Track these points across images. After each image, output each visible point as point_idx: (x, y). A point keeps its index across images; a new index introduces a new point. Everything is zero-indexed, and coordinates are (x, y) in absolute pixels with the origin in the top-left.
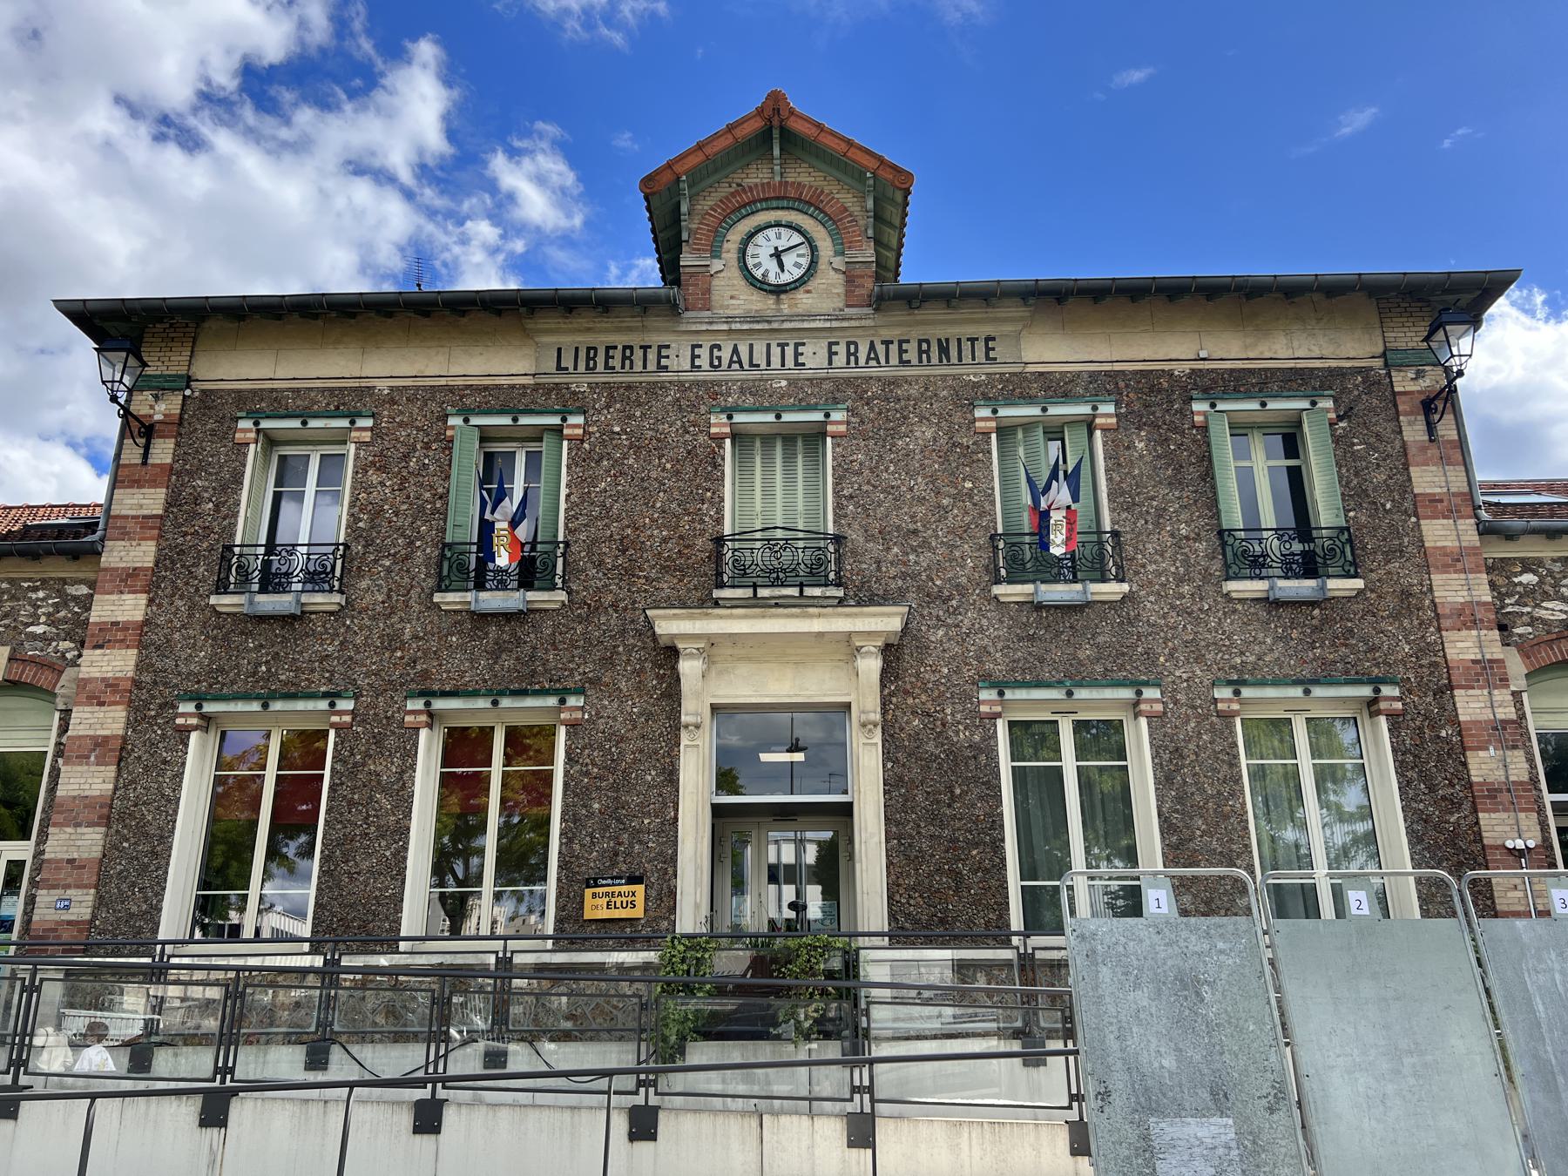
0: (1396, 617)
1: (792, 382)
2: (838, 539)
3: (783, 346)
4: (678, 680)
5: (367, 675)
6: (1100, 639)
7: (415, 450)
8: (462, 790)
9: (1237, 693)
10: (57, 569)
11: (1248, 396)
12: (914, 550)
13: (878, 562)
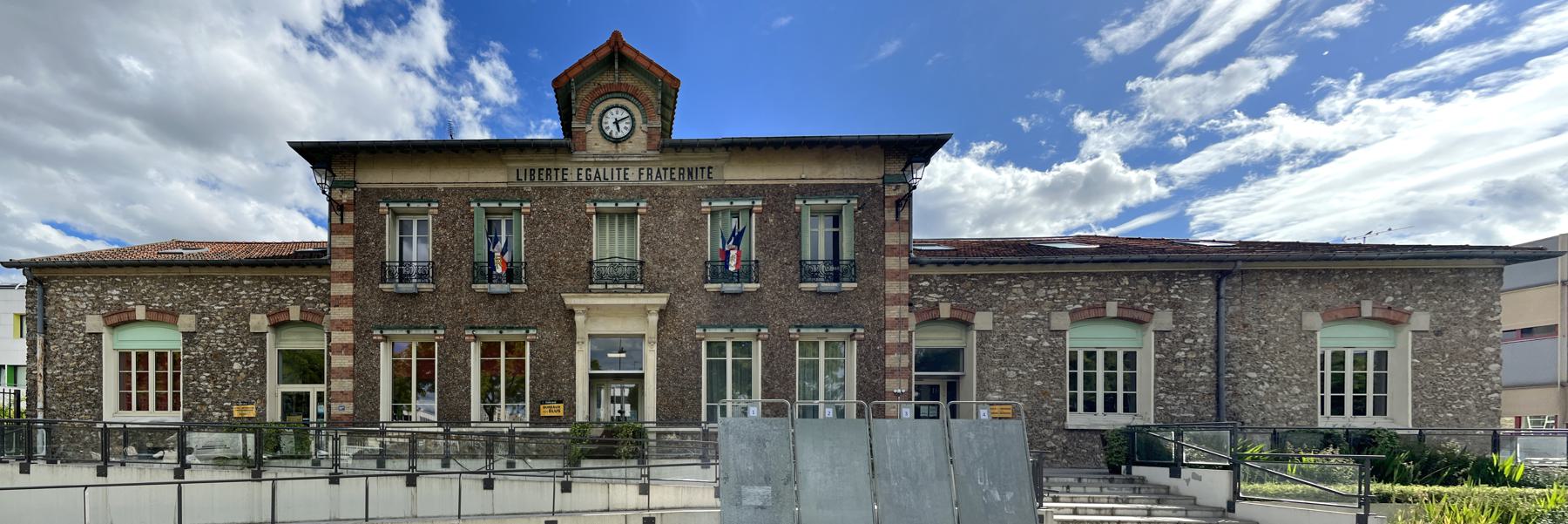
0: (868, 299)
1: (623, 188)
2: (642, 263)
8: (489, 367)
10: (315, 272)
11: (820, 198)
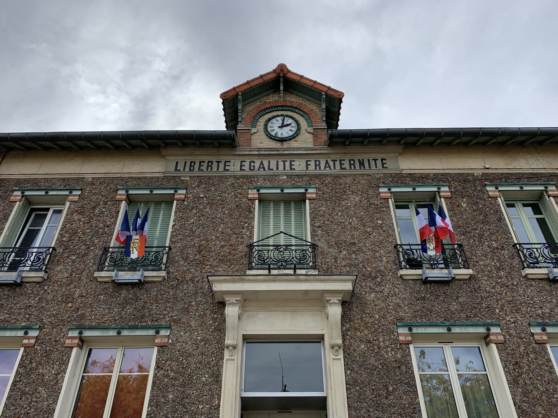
2: (314, 246)
3: (284, 162)
4: (225, 321)
5: (50, 316)
6: (461, 300)
7: (99, 205)
9: (544, 330)
12: (354, 252)
13: (336, 259)
